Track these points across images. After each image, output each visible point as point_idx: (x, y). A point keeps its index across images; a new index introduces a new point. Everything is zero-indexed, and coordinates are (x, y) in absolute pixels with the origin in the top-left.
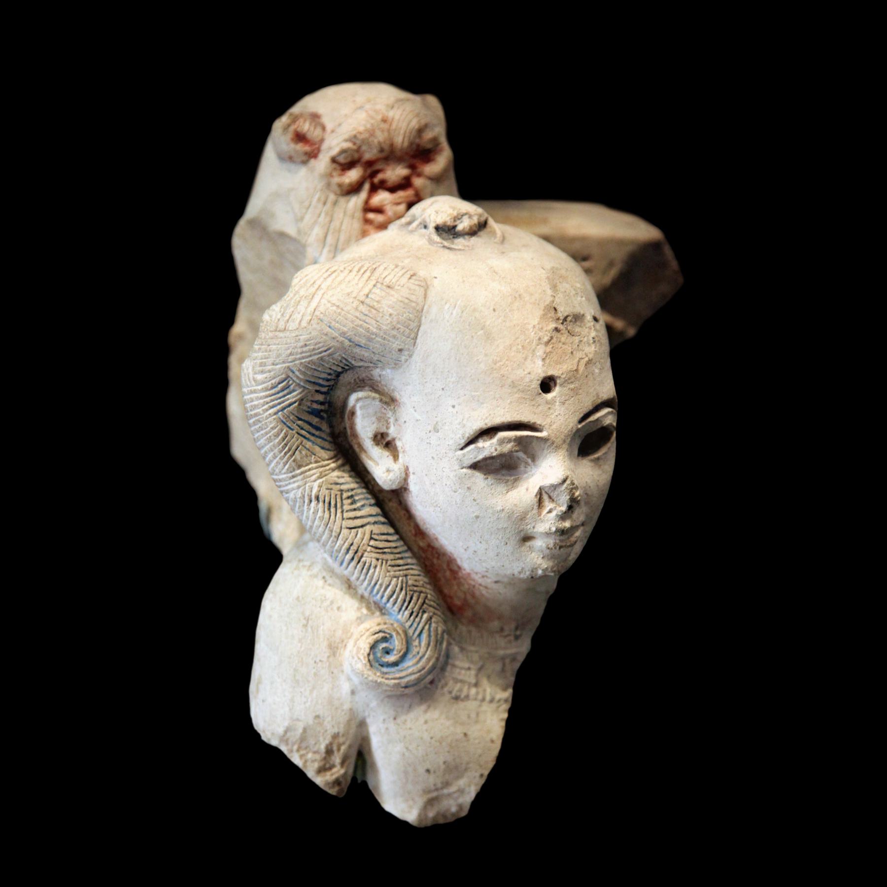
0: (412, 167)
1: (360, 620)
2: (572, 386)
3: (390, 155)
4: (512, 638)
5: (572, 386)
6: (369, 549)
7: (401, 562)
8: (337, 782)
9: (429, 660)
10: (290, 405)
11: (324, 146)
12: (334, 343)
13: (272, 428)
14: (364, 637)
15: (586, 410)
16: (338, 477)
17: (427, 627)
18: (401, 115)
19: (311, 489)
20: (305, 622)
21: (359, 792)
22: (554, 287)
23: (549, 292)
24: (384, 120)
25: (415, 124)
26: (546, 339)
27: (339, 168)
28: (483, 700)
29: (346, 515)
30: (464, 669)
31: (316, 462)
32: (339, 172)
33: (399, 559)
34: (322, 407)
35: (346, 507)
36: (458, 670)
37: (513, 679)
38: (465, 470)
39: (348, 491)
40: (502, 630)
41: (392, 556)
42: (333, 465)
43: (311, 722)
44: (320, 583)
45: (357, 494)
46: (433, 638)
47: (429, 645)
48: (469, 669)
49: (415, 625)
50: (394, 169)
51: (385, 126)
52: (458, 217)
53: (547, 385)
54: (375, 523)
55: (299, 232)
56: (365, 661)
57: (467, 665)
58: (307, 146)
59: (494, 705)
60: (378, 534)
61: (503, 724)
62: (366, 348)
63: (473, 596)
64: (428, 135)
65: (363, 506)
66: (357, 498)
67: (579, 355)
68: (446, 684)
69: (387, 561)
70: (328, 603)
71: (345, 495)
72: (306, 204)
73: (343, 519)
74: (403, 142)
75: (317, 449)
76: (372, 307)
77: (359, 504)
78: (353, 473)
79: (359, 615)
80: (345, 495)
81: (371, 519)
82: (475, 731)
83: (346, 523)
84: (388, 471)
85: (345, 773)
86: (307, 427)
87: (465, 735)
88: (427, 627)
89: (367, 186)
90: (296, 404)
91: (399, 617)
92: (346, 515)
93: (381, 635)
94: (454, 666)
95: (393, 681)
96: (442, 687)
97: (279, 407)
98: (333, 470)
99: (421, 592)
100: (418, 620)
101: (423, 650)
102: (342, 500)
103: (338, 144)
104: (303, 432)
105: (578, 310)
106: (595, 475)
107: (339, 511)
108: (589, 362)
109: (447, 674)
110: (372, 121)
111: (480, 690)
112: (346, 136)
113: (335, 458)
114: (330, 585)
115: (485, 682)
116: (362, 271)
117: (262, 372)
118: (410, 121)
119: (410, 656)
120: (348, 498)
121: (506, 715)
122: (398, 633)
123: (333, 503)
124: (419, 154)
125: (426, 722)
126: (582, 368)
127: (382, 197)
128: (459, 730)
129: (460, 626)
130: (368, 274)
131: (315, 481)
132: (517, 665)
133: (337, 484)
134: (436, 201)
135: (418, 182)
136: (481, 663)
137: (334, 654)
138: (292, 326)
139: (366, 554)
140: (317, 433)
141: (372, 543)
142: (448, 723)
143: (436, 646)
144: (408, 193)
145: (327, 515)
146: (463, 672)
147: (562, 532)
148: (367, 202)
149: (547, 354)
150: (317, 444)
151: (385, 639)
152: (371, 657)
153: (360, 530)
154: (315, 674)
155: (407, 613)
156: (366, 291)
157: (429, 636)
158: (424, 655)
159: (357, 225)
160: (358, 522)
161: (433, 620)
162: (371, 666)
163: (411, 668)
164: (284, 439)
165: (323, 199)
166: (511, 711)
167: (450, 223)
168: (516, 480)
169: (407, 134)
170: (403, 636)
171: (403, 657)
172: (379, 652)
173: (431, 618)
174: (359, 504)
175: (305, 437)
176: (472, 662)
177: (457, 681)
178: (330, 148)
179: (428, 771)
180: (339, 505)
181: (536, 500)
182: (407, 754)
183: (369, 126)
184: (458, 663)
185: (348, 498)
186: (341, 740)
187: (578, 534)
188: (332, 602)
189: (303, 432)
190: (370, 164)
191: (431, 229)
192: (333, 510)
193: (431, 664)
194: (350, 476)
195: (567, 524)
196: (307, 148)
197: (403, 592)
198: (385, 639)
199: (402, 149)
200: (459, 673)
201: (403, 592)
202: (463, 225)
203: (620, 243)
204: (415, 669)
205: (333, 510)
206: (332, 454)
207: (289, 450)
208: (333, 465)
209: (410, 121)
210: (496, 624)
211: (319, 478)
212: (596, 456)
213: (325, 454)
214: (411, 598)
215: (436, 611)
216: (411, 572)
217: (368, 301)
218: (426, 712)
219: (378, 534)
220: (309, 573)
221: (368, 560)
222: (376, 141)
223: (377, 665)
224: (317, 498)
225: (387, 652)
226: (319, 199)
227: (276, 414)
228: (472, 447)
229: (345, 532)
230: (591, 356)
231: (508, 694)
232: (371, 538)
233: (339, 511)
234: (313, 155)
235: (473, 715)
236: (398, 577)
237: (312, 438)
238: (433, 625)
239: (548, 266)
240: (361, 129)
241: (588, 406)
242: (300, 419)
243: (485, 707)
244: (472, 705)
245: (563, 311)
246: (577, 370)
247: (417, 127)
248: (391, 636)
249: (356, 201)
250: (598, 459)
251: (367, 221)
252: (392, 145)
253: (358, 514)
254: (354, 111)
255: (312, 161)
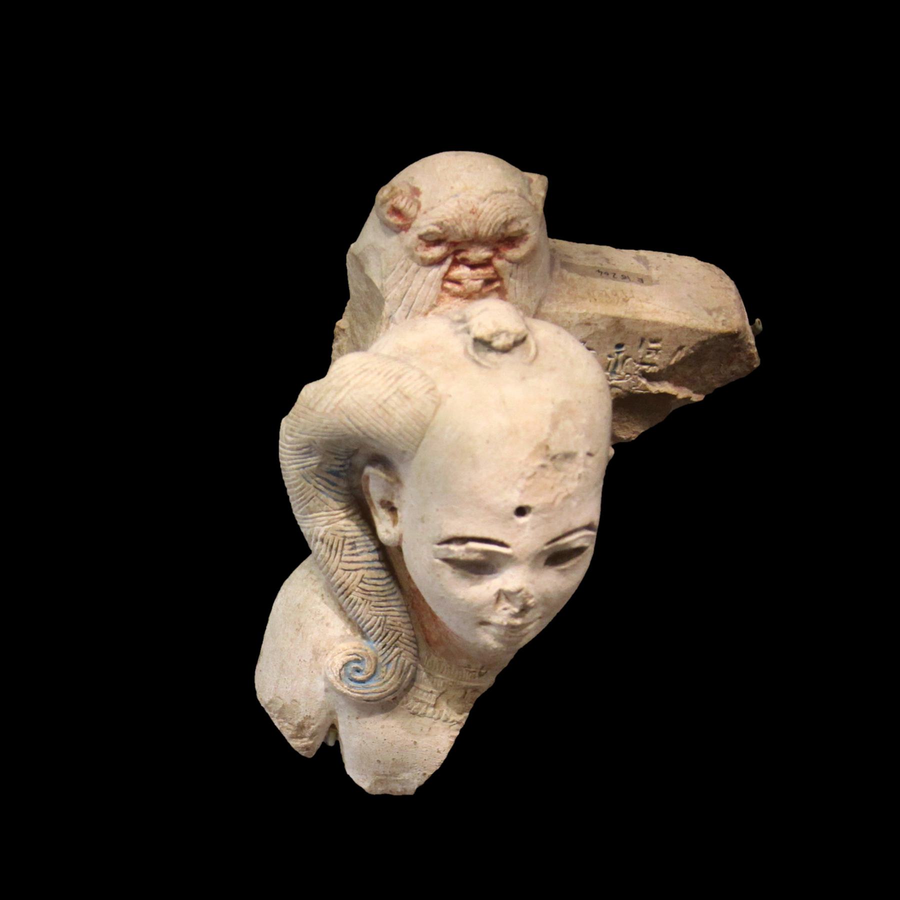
0: (496, 250)
1: (343, 639)
2: (545, 516)
3: (476, 240)
4: (477, 674)
5: (545, 516)
6: (357, 589)
7: (384, 604)
8: (307, 748)
9: (391, 685)
10: (310, 465)
11: (414, 225)
12: (349, 432)
13: (293, 479)
14: (340, 655)
15: (554, 536)
16: (345, 525)
17: (396, 659)
18: (491, 209)
19: (319, 532)
20: (298, 627)
21: (331, 754)
22: (555, 425)
23: (547, 429)
24: (473, 212)
25: (502, 217)
26: (529, 474)
27: (424, 243)
28: (439, 718)
29: (343, 558)
30: (426, 691)
31: (327, 511)
32: (424, 247)
33: (383, 601)
34: (342, 469)
35: (345, 552)
36: (420, 692)
37: (471, 705)
38: (437, 561)
39: (352, 537)
40: (469, 666)
41: (377, 599)
42: (343, 515)
43: (288, 703)
44: (319, 599)
45: (358, 542)
46: (399, 669)
47: (394, 673)
48: (431, 692)
49: (386, 655)
50: (475, 252)
51: (473, 217)
52: (497, 334)
53: (521, 511)
54: (369, 568)
55: (382, 286)
56: (337, 675)
57: (430, 689)
58: (401, 222)
59: (447, 724)
60: (368, 579)
61: (453, 740)
62: (378, 442)
63: (447, 638)
64: (514, 228)
65: (362, 552)
66: (358, 545)
67: (558, 489)
68: (407, 702)
69: (371, 602)
70: (320, 617)
71: (347, 541)
72: (392, 266)
73: (340, 561)
74: (487, 232)
75: (330, 501)
76: (387, 412)
77: (358, 550)
78: (361, 522)
79: (343, 633)
80: (347, 541)
81: (366, 565)
82: (423, 742)
83: (342, 565)
84: (387, 531)
85: (313, 744)
86: (324, 483)
87: (415, 743)
88: (396, 659)
89: (449, 261)
90: (315, 466)
91: (374, 645)
92: (343, 558)
93: (355, 657)
94: (418, 688)
95: (357, 695)
96: (403, 704)
97: (301, 465)
98: (342, 519)
99: (396, 631)
100: (389, 651)
101: (388, 676)
102: (343, 545)
103: (425, 226)
104: (320, 487)
105: (572, 448)
106: (561, 583)
107: (339, 553)
108: (568, 496)
109: (409, 694)
110: (462, 212)
111: (437, 710)
112: (434, 221)
113: (347, 508)
114: (325, 603)
115: (443, 704)
116: (388, 377)
117: (291, 436)
118: (498, 215)
119: (375, 678)
120: (350, 544)
121: (457, 733)
122: (369, 658)
123: (334, 546)
124: (504, 240)
125: (383, 727)
126: (558, 501)
127: (462, 271)
128: (410, 739)
129: (433, 656)
130: (393, 380)
131: (323, 526)
132: (478, 695)
133: (342, 531)
134: (486, 309)
135: (498, 263)
136: (444, 689)
137: (316, 659)
138: (319, 409)
139: (354, 593)
140: (333, 488)
141: (362, 585)
142: (402, 731)
143: (400, 675)
144: (488, 272)
145: (327, 555)
146: (425, 694)
147: (512, 627)
148: (446, 274)
149: (527, 488)
150: (330, 496)
151: (357, 661)
152: (343, 672)
153: (353, 573)
154: (298, 669)
155: (381, 644)
156: (385, 396)
157: (396, 666)
158: (387, 681)
159: (433, 292)
160: (353, 566)
161: (403, 654)
162: (341, 679)
163: (374, 689)
164: (301, 489)
165: (405, 266)
166: (462, 731)
167: (486, 338)
168: (479, 579)
169: (493, 226)
170: (373, 662)
171: (369, 679)
172: (351, 668)
173: (401, 652)
174: (358, 550)
175: (320, 490)
176: (436, 687)
177: (417, 701)
178: (418, 228)
179: (379, 761)
180: (339, 549)
181: (494, 598)
182: (363, 746)
183: (456, 216)
184: (422, 686)
185: (350, 544)
186: (311, 721)
187: (531, 627)
188: (323, 618)
189: (320, 487)
190: (454, 244)
191: (469, 339)
192: (333, 552)
193: (392, 688)
194: (357, 525)
195: (518, 622)
196: (400, 222)
197: (380, 629)
198: (357, 661)
199: (485, 237)
200: (422, 695)
201: (380, 629)
202: (498, 343)
203: (692, 331)
204: (378, 689)
205: (333, 552)
206: (343, 505)
207: (305, 499)
208: (343, 515)
209: (498, 215)
210: (464, 662)
211: (327, 524)
212: (563, 567)
213: (336, 505)
214: (387, 634)
215: (407, 647)
216: (392, 613)
217: (385, 406)
218: (384, 719)
219: (368, 579)
220: (313, 587)
221: (355, 598)
222: (460, 230)
223: (347, 679)
224: (322, 540)
225: (358, 671)
226: (402, 266)
227: (298, 469)
228: (445, 546)
229: (340, 571)
230: (571, 491)
231: (463, 717)
232: (361, 581)
233: (339, 553)
234: (405, 228)
235: (426, 729)
236: (378, 616)
237: (327, 492)
238: (402, 658)
239: (560, 399)
240: (449, 217)
241: (558, 532)
242: (318, 476)
243: (439, 724)
244: (425, 720)
245: (556, 449)
246: (553, 503)
247: (503, 221)
248: (363, 660)
249: (437, 272)
250: (564, 570)
251: (443, 289)
252: (476, 233)
253: (355, 558)
254: (461, 186)
255: (403, 232)
